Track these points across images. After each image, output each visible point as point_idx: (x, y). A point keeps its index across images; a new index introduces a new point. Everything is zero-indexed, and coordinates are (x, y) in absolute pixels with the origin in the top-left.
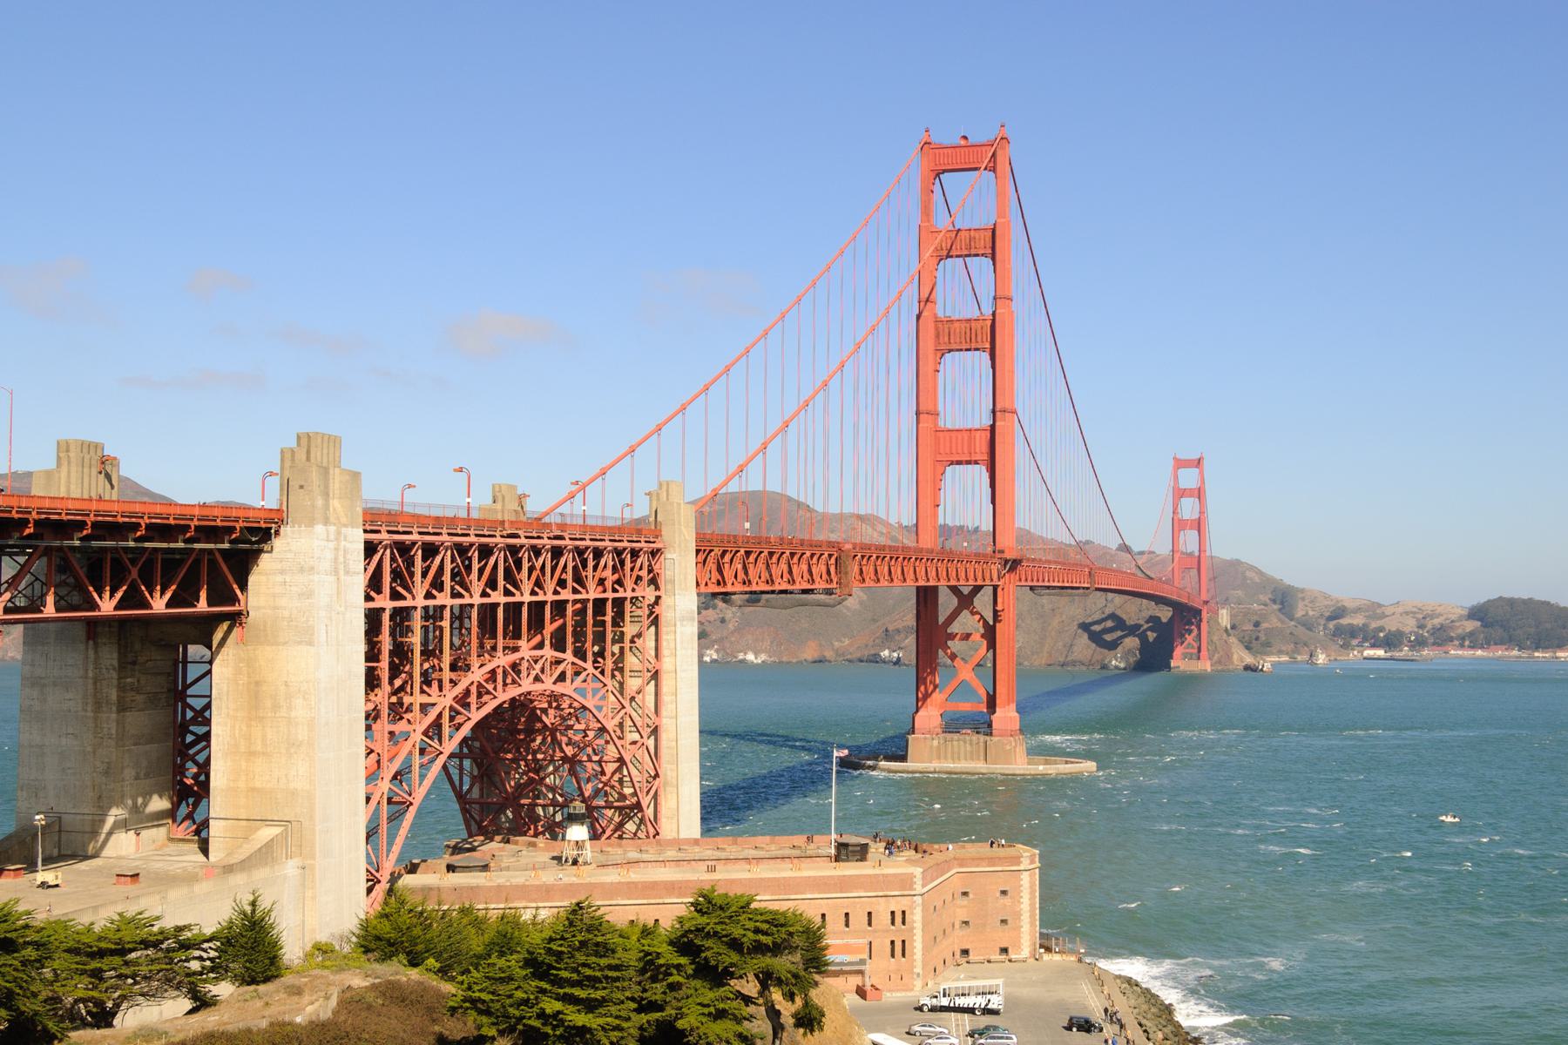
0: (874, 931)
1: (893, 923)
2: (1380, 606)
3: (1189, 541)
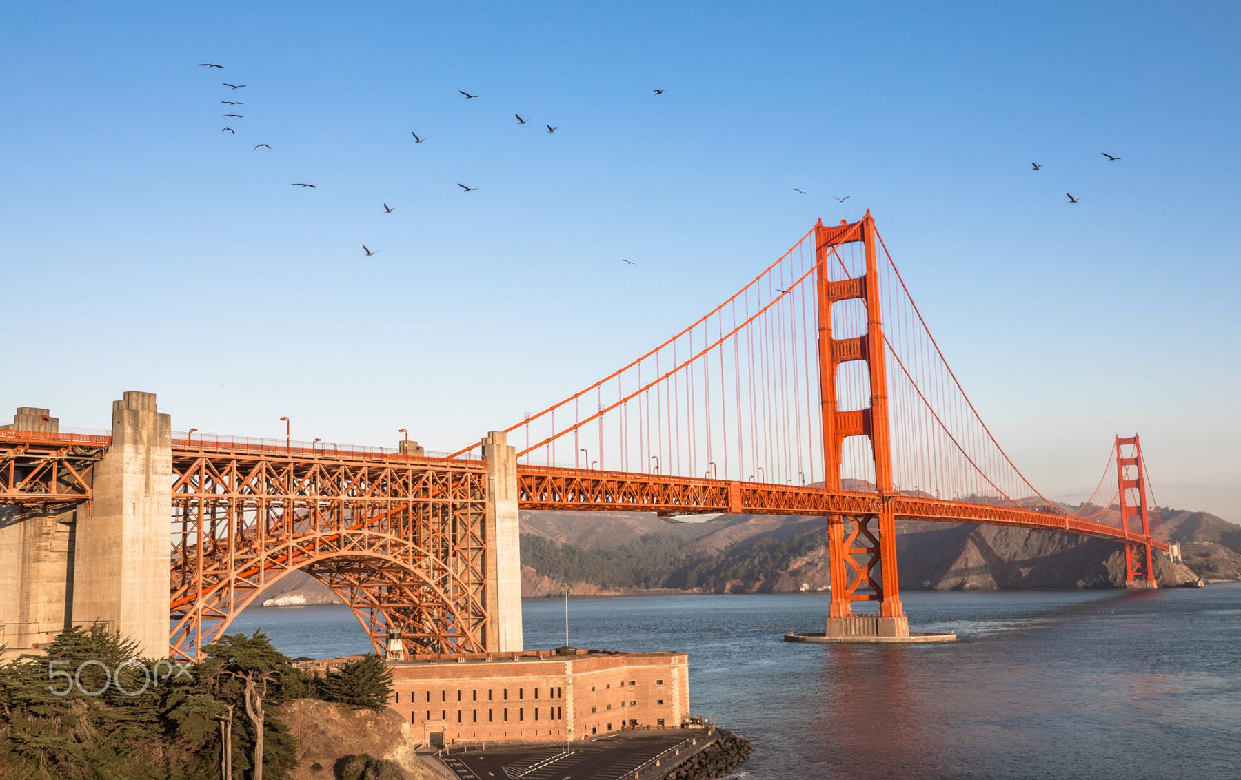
0: (540, 701)
1: (552, 697)
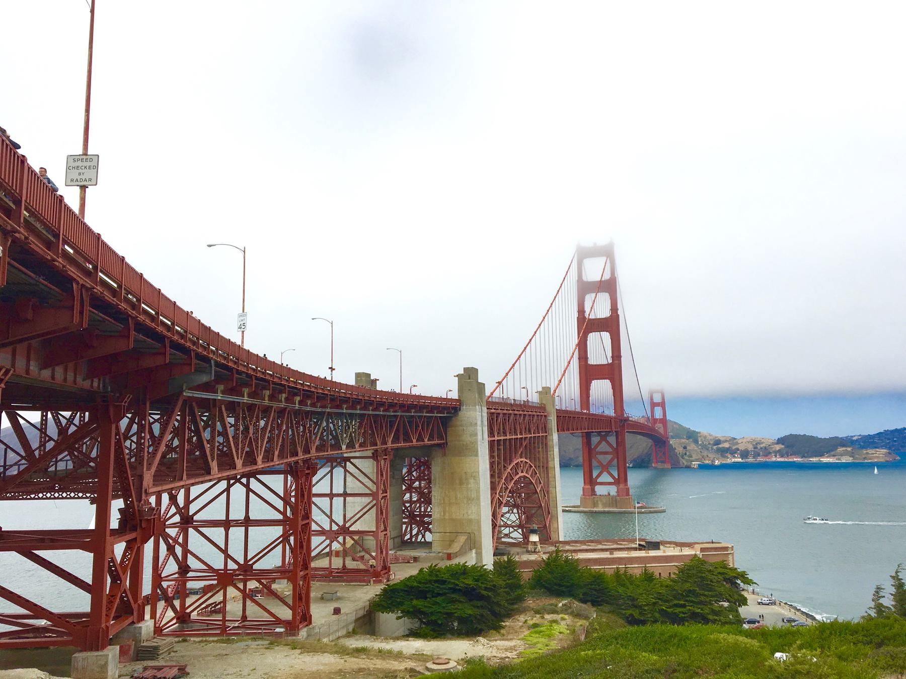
2: (735, 439)
3: (658, 413)
